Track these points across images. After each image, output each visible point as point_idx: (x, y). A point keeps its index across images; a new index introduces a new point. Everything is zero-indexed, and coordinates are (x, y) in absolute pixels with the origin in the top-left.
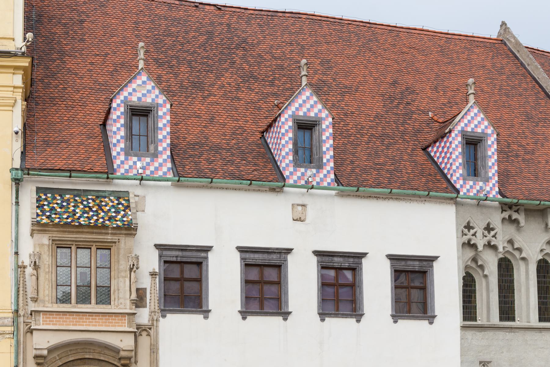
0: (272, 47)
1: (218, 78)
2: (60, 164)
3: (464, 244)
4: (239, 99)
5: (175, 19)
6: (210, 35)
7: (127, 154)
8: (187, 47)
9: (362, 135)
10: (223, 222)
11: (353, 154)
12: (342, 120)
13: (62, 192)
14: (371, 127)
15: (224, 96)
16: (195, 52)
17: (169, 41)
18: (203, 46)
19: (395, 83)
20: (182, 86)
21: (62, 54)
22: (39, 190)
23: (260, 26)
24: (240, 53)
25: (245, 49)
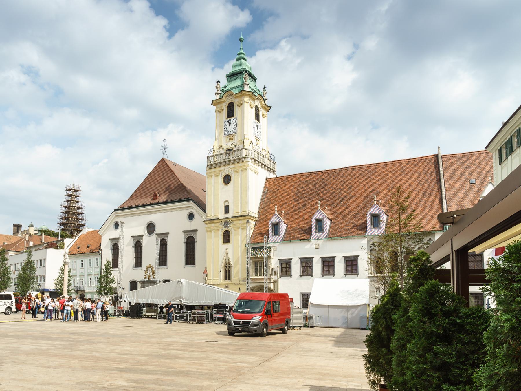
0: (334, 185)
1: (311, 202)
2: (257, 241)
3: (371, 250)
4: (314, 209)
5: (307, 181)
6: (316, 184)
7: (273, 236)
8: (307, 192)
9: (349, 215)
10: (295, 252)
11: (341, 224)
12: (345, 210)
13: (256, 248)
14: (354, 211)
15: (311, 209)
16: (308, 193)
17: (301, 191)
18: (311, 190)
19: (373, 190)
20: (299, 208)
21: (270, 203)
22: (252, 248)
23: (334, 176)
24: (322, 190)
25: (325, 188)
